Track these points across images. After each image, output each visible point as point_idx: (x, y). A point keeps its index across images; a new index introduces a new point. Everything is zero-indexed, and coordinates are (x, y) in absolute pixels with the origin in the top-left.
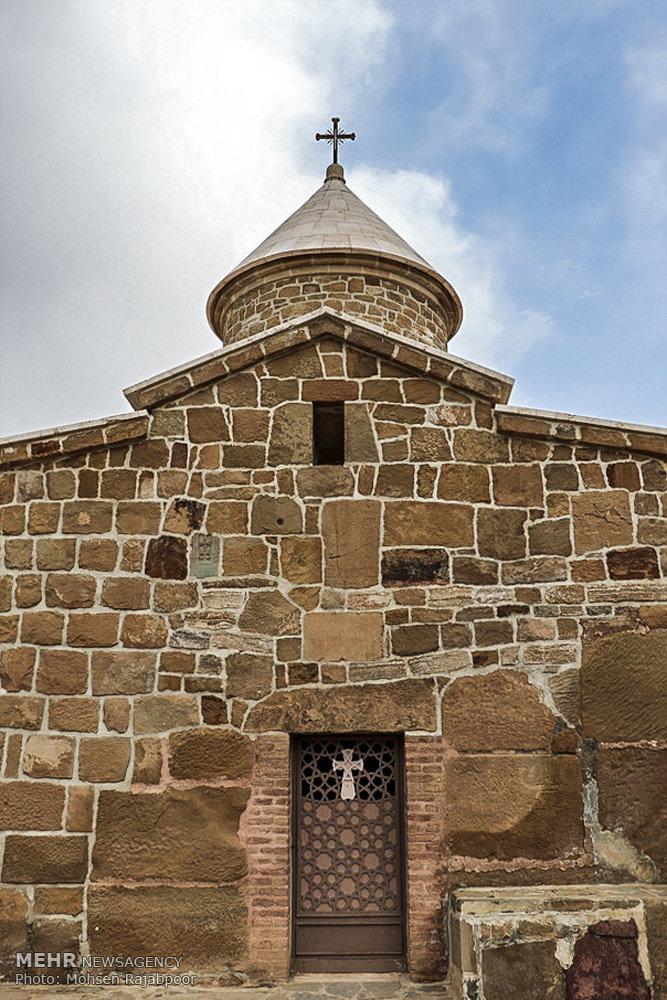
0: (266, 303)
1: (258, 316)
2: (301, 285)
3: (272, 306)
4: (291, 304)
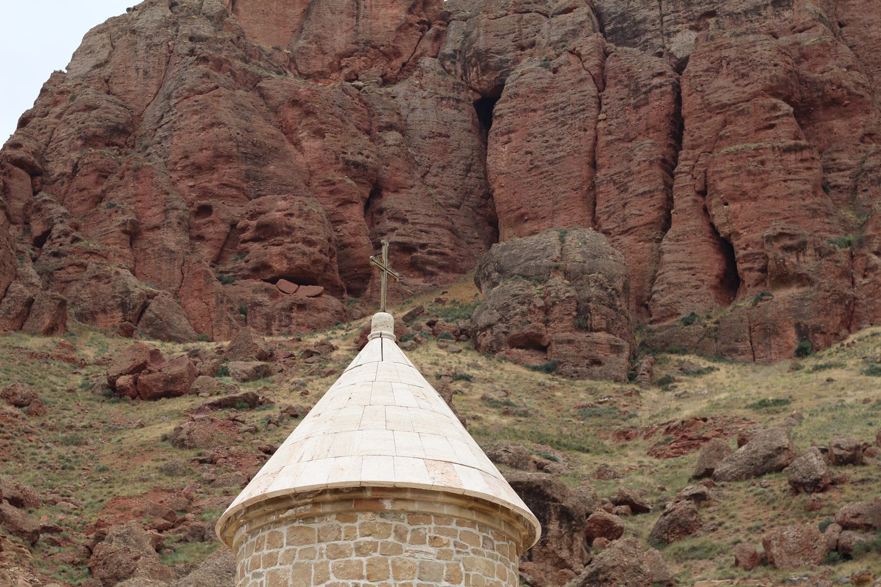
0: (445, 539)
1: (432, 550)
2: (481, 535)
3: (452, 547)
4: (472, 555)
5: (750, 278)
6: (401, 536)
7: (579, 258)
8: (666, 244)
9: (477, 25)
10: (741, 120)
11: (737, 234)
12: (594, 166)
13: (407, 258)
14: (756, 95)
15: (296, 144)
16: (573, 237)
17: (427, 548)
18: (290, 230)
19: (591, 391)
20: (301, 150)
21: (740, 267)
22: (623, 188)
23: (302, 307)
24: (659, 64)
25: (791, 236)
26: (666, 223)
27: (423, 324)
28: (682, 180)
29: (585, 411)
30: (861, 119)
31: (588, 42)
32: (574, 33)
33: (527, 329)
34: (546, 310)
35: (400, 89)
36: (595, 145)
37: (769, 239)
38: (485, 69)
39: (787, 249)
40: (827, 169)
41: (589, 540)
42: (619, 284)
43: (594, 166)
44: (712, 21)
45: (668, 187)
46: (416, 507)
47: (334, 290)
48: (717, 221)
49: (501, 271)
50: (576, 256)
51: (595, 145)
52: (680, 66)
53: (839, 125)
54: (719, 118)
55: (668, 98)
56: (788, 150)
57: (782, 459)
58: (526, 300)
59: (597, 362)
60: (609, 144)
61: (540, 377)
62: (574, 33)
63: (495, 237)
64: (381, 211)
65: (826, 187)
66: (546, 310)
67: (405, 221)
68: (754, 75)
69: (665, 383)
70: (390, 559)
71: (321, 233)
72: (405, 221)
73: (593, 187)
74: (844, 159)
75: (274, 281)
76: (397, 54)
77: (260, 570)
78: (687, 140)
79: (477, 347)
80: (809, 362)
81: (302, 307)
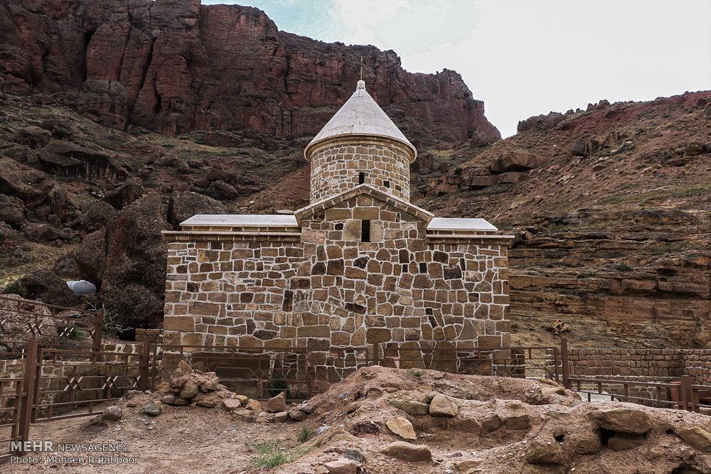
5: (165, 108)
6: (395, 157)
7: (114, 90)
8: (140, 93)
9: (90, 9)
10: (170, 60)
11: (163, 95)
12: (121, 63)
13: (55, 77)
14: (176, 54)
15: (20, 30)
16: (113, 83)
17: (400, 163)
18: (15, 58)
19: (113, 132)
20: (22, 33)
21: (162, 104)
22: (130, 72)
23: (16, 85)
24: (148, 37)
25: (179, 98)
26: (141, 86)
27: (59, 99)
28: (149, 74)
29: (111, 138)
30: (205, 69)
31: (126, 24)
32: (122, 20)
33: (94, 108)
34: (101, 104)
35: (60, 22)
36: (123, 57)
37: (173, 98)
38: (91, 23)
39: (177, 102)
40: (192, 81)
41: (117, 176)
42: (126, 101)
43: (121, 63)
44: (166, 28)
45: (144, 76)
46: (399, 149)
47: (27, 81)
48: (158, 89)
49: (88, 89)
50: (114, 90)
51: (123, 57)
52: (154, 39)
53: (198, 69)
54: (164, 58)
55: (148, 48)
56: (183, 73)
57: (175, 163)
58: (96, 99)
59: (115, 123)
60: (127, 57)
61: (97, 125)
62: (122, 20)
63: (84, 78)
64: (48, 60)
65: (192, 87)
66: (101, 104)
67: (56, 65)
68: (177, 48)
69: (135, 135)
70: (393, 164)
71: (26, 62)
72: (56, 65)
73: (120, 69)
74: (198, 80)
75: (6, 74)
76: (60, 10)
77: (343, 160)
78: (152, 62)
79: (77, 111)
80: (179, 137)
81: (16, 85)
